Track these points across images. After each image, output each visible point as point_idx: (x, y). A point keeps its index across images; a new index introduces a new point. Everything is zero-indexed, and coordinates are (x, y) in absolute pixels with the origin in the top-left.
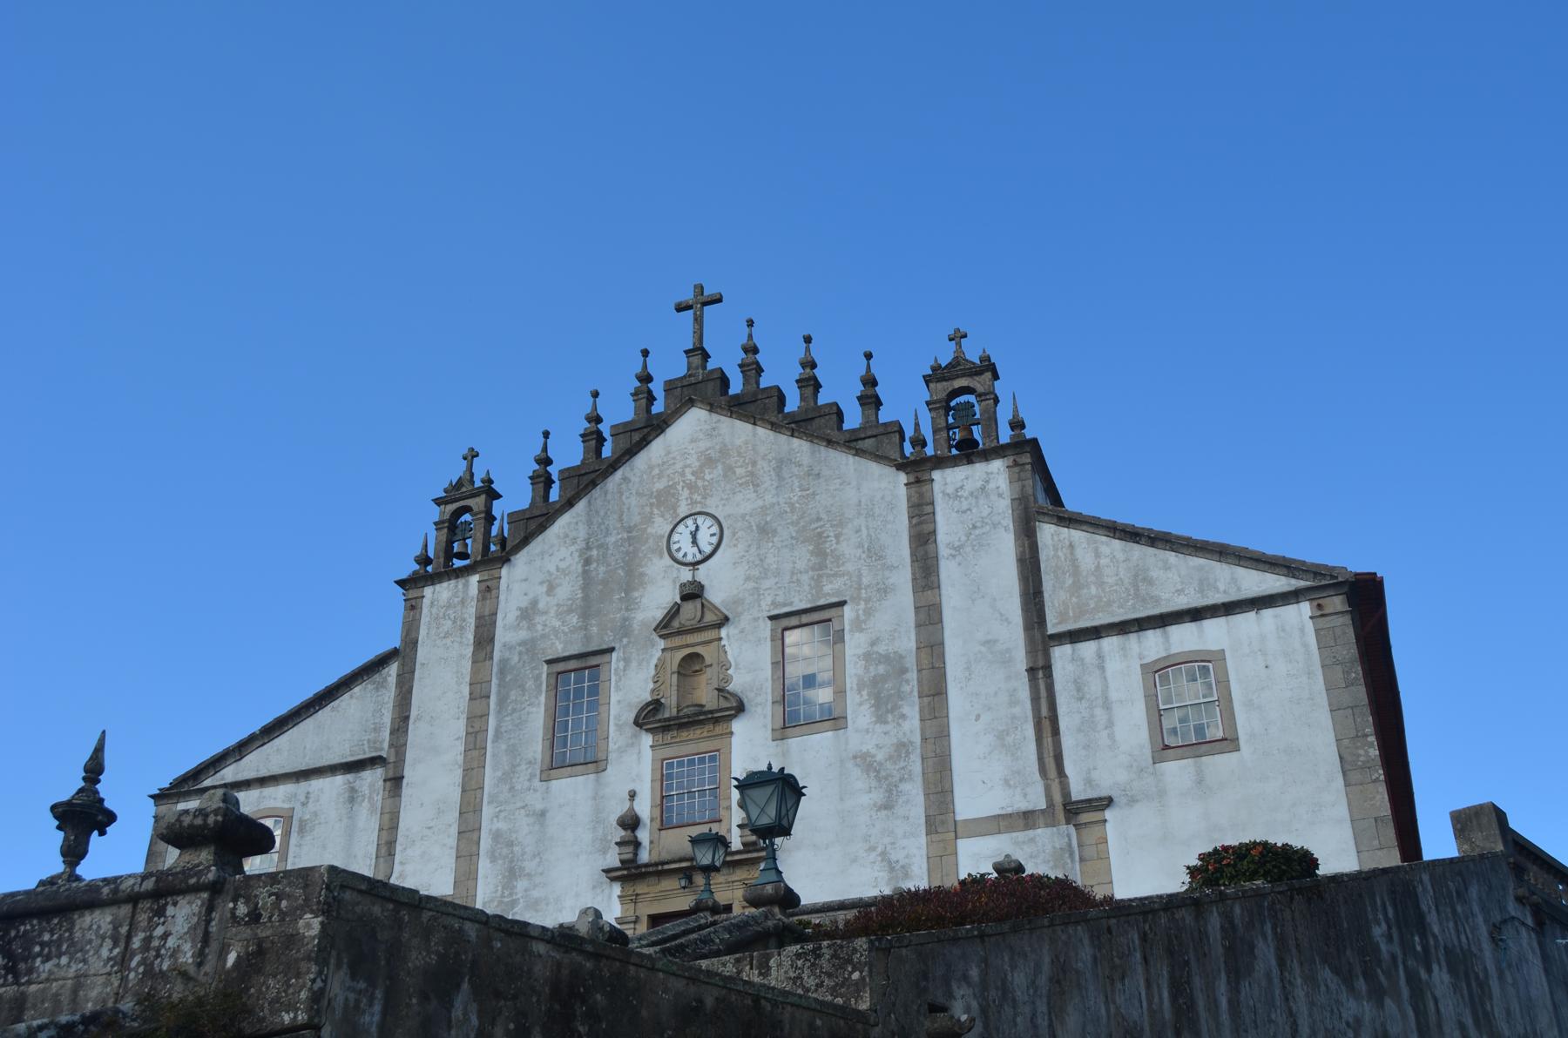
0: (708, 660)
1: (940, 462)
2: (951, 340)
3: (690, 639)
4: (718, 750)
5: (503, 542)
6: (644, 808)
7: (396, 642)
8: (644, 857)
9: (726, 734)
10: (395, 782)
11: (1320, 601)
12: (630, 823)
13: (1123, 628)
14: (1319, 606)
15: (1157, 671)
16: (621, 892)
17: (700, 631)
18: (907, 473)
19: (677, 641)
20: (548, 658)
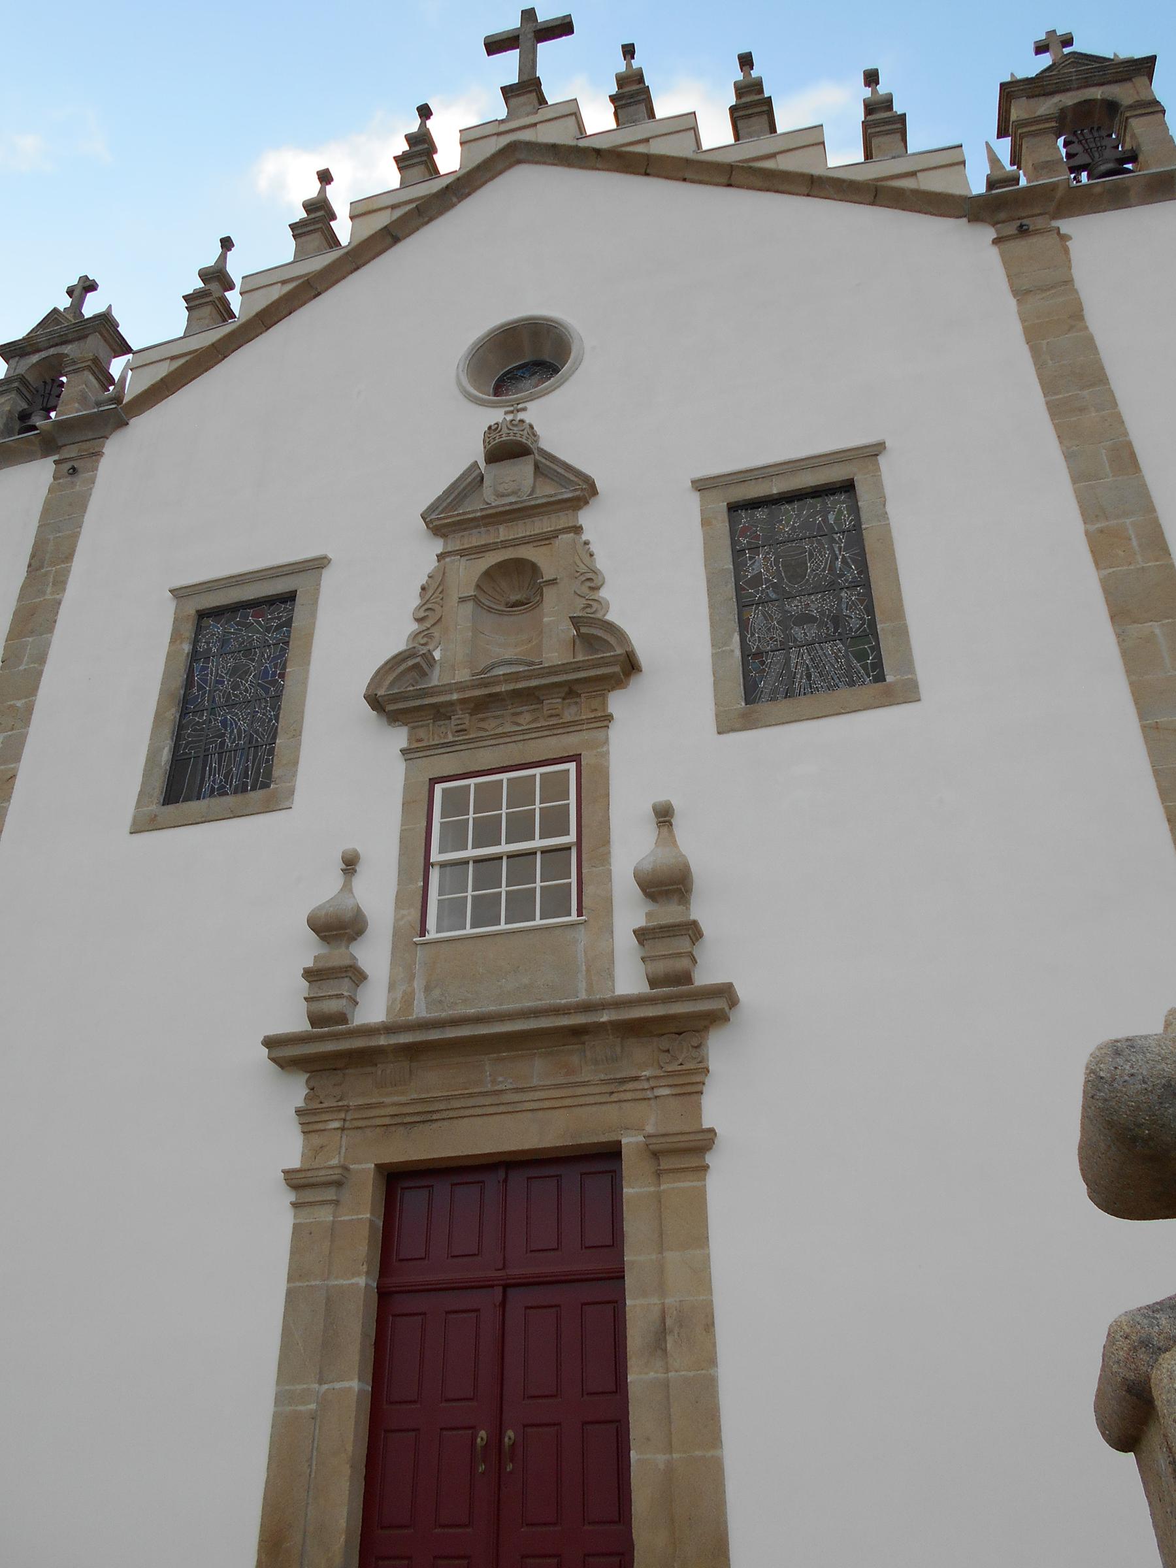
0: (548, 573)
3: (504, 533)
4: (576, 758)
9: (597, 719)
16: (307, 1098)
17: (530, 516)
19: (476, 538)
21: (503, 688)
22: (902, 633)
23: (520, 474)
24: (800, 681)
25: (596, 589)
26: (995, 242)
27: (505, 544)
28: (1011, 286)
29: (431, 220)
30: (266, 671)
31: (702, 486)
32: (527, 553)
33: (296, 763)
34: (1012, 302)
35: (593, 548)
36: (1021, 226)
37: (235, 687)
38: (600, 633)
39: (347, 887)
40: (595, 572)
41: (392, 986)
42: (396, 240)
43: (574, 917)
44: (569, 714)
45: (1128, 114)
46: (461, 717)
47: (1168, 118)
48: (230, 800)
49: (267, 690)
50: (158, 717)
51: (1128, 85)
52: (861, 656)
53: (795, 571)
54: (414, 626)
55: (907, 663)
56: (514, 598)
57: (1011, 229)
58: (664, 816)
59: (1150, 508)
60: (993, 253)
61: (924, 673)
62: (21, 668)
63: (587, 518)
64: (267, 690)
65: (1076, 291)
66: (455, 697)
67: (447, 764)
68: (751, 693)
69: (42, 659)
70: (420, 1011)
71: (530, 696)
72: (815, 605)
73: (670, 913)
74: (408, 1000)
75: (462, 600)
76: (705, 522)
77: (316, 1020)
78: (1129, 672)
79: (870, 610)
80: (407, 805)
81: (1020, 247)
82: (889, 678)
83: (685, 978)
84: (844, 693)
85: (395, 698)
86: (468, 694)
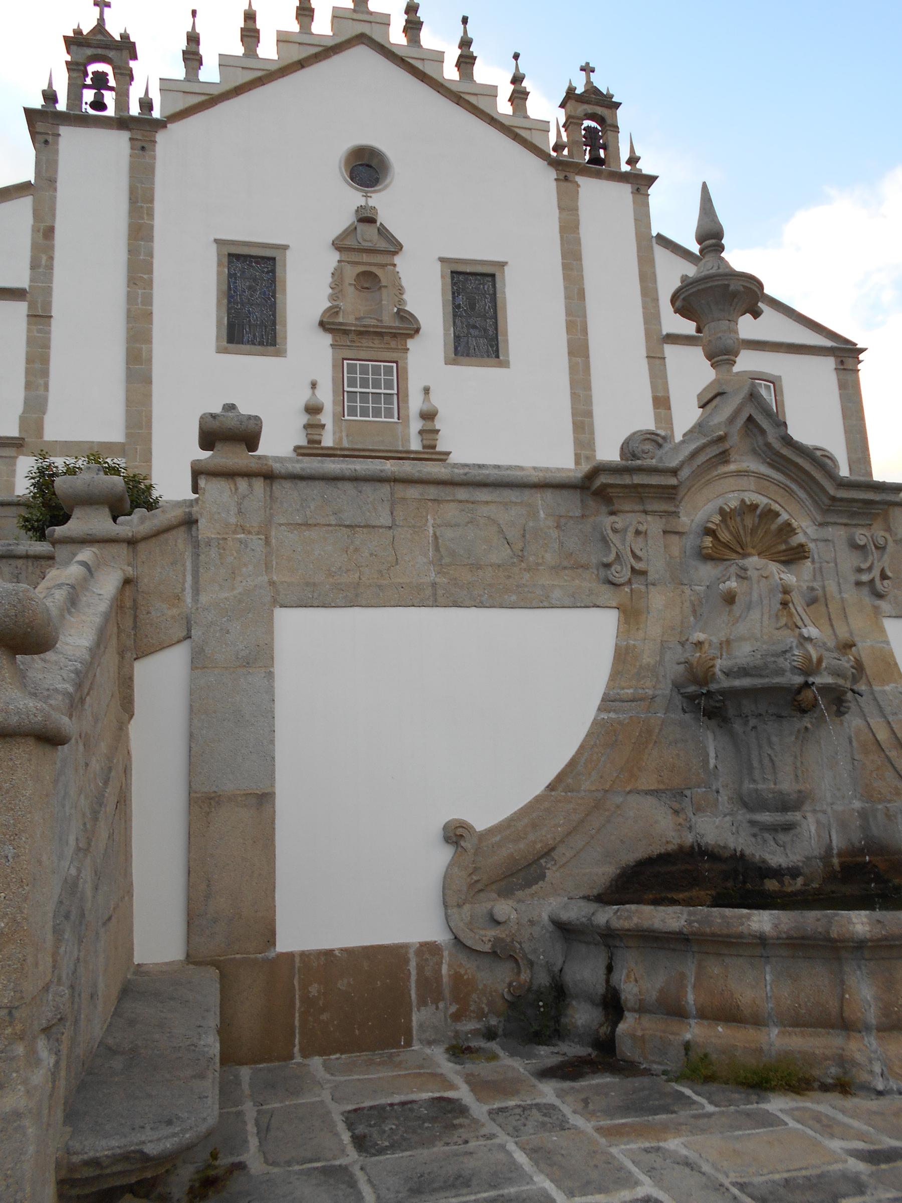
0: (384, 283)
1: (583, 170)
3: (365, 258)
4: (396, 362)
5: (146, 104)
6: (326, 396)
7: (28, 174)
8: (328, 441)
12: (313, 409)
14: (842, 362)
18: (556, 170)
19: (354, 257)
20: (218, 237)
21: (372, 330)
22: (506, 341)
24: (472, 351)
25: (401, 294)
26: (556, 180)
28: (559, 204)
29: (320, 61)
30: (265, 294)
31: (442, 260)
32: (374, 269)
33: (286, 338)
34: (557, 211)
35: (401, 275)
36: (566, 176)
38: (408, 317)
39: (314, 394)
40: (402, 287)
41: (334, 433)
42: (303, 67)
43: (396, 420)
44: (393, 344)
45: (608, 128)
46: (352, 336)
47: (619, 135)
49: (267, 302)
51: (610, 111)
52: (492, 347)
53: (472, 306)
54: (330, 291)
55: (507, 355)
56: (365, 285)
57: (562, 177)
58: (427, 390)
59: (585, 316)
60: (554, 184)
61: (512, 358)
63: (397, 260)
64: (267, 302)
65: (578, 215)
66: (353, 328)
67: (348, 353)
68: (456, 352)
69: (151, 255)
70: (345, 444)
72: (478, 322)
73: (429, 426)
74: (341, 439)
75: (350, 284)
76: (442, 277)
77: (309, 442)
78: (570, 373)
79: (496, 329)
80: (334, 366)
81: (564, 184)
82: (501, 358)
83: (434, 447)
84: (486, 360)
85: (329, 323)
86: (359, 329)
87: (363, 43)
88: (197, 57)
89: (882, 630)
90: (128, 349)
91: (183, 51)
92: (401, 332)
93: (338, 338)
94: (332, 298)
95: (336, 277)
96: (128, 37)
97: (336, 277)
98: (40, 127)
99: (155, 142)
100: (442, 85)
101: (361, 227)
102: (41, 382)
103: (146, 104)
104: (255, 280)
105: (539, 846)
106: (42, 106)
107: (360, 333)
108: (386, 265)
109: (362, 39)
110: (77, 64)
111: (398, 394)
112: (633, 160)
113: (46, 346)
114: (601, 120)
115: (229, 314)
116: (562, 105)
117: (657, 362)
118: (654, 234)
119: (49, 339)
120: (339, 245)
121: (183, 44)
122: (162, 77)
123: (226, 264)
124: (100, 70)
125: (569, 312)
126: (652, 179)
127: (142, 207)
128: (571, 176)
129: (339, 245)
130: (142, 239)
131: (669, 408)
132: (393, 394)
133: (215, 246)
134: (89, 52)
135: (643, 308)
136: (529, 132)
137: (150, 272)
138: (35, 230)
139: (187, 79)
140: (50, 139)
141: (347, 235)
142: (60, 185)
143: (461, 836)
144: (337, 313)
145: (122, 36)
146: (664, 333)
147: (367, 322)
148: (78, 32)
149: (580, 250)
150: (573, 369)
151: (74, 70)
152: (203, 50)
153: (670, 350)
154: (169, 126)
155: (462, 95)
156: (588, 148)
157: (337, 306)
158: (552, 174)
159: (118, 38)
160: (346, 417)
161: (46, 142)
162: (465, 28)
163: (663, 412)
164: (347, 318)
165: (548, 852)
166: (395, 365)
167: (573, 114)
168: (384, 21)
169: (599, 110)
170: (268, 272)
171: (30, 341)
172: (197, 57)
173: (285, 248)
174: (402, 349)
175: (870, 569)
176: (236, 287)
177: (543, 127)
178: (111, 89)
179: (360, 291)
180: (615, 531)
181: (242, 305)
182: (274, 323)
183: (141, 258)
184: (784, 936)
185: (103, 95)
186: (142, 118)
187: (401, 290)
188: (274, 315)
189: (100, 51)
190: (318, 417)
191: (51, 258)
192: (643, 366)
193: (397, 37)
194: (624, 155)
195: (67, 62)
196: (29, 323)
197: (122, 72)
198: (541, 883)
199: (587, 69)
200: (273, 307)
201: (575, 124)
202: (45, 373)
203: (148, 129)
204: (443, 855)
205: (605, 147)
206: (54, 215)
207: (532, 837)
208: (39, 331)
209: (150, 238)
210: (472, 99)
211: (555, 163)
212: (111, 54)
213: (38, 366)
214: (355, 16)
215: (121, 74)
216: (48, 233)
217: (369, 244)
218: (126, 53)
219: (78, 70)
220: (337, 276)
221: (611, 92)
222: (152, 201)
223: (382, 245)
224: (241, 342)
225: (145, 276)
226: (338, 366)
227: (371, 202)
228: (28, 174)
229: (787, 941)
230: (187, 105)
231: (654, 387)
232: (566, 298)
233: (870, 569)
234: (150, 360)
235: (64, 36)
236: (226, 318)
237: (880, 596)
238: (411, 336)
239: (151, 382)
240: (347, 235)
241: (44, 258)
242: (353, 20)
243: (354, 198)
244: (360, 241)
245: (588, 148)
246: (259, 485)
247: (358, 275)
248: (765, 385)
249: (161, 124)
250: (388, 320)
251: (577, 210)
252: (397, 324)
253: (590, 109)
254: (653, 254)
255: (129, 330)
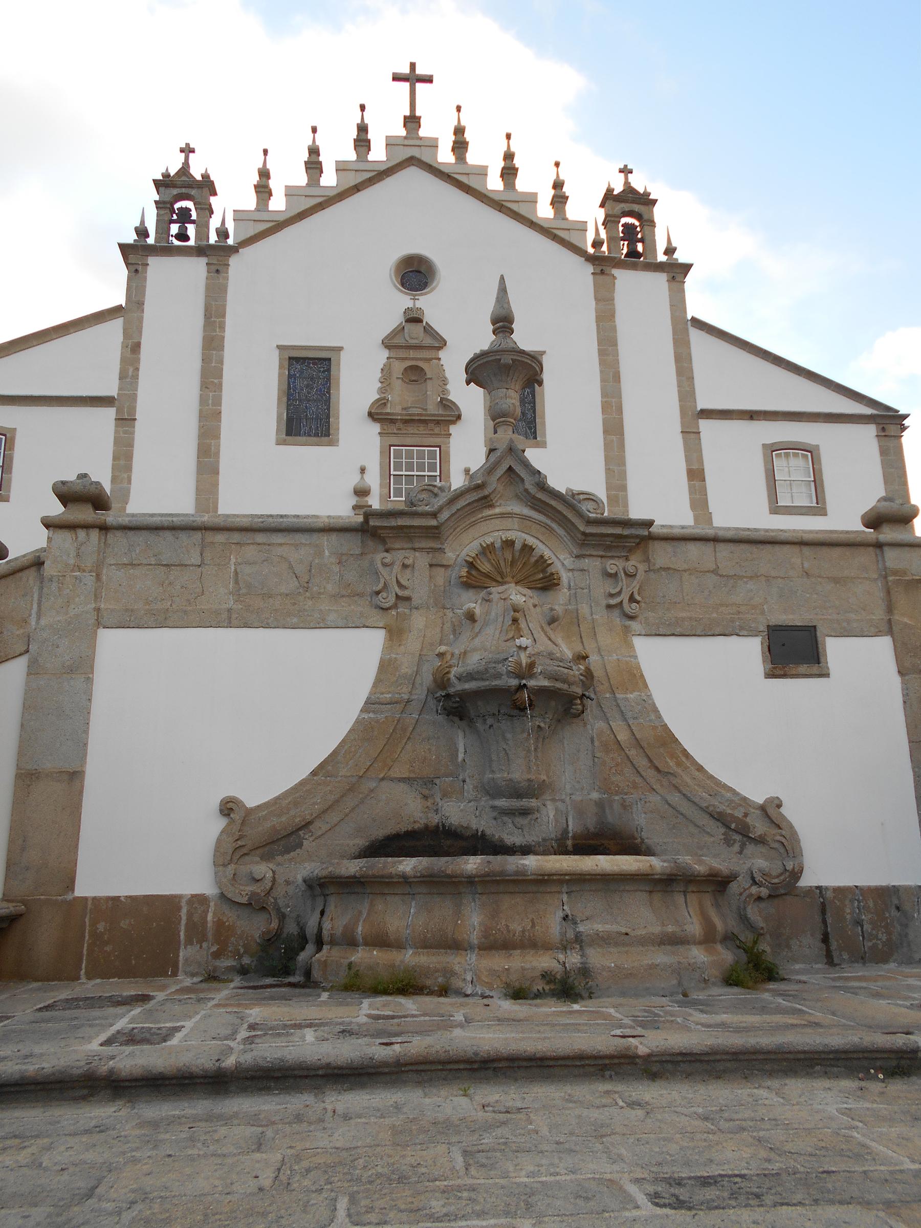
2: (620, 172)
3: (412, 354)
4: (439, 447)
5: (223, 233)
6: (373, 480)
7: (120, 299)
9: (446, 434)
10: (126, 420)
11: (884, 426)
13: (752, 415)
15: (772, 450)
19: (402, 354)
21: (417, 418)
22: (544, 424)
23: (417, 329)
25: (446, 385)
27: (413, 359)
28: (595, 296)
32: (420, 364)
34: (594, 303)
35: (445, 367)
37: (309, 393)
38: (450, 405)
39: (362, 478)
44: (437, 430)
48: (315, 439)
49: (322, 397)
50: (279, 399)
52: (530, 428)
54: (380, 385)
55: (544, 435)
56: (413, 378)
57: (598, 271)
60: (591, 277)
61: (549, 439)
62: (213, 365)
63: (441, 354)
67: (394, 440)
69: (221, 362)
71: (425, 422)
75: (397, 378)
78: (605, 451)
85: (377, 414)
86: (404, 418)
87: (413, 165)
88: (266, 190)
89: (631, 646)
90: (199, 444)
91: (255, 185)
92: (443, 418)
93: (385, 427)
94: (381, 390)
95: (385, 372)
96: (208, 177)
97: (385, 372)
98: (132, 258)
99: (228, 265)
100: (485, 196)
101: (409, 327)
102: (126, 476)
103: (223, 233)
104: (312, 379)
105: (297, 820)
106: (135, 240)
107: (406, 422)
108: (431, 359)
109: (412, 161)
110: (164, 202)
111: (440, 476)
112: (670, 251)
113: (130, 445)
114: (638, 217)
115: (288, 410)
116: (602, 205)
117: (693, 436)
118: (689, 318)
119: (133, 439)
120: (388, 343)
121: (256, 178)
122: (235, 209)
123: (287, 366)
124: (184, 206)
125: (604, 394)
126: (687, 268)
127: (215, 322)
128: (606, 269)
129: (388, 343)
130: (214, 349)
131: (704, 480)
132: (436, 476)
133: (277, 352)
134: (175, 191)
135: (679, 386)
136: (567, 232)
137: (220, 376)
138: (124, 346)
139: (258, 210)
140: (140, 268)
141: (395, 335)
142: (147, 307)
143: (232, 809)
144: (385, 404)
145: (202, 176)
146: (699, 409)
147: (412, 411)
148: (166, 175)
149: (616, 337)
150: (607, 446)
151: (161, 208)
152: (272, 183)
153: (705, 425)
154: (240, 250)
155: (504, 203)
156: (626, 243)
157: (384, 398)
158: (590, 269)
159: (199, 178)
160: (392, 498)
161: (136, 271)
162: (508, 142)
163: (697, 483)
164: (394, 409)
165: (307, 824)
166: (438, 449)
167: (610, 213)
168: (433, 145)
169: (636, 208)
170: (324, 372)
171: (117, 441)
172: (266, 190)
173: (339, 349)
174: (444, 435)
175: (620, 593)
176: (295, 386)
177: (581, 227)
178: (193, 222)
179: (407, 383)
180: (385, 565)
181: (300, 401)
182: (328, 417)
183: (213, 365)
184: (419, 875)
185: (186, 228)
186: (218, 246)
187: (445, 382)
188: (329, 409)
189: (184, 190)
190: (366, 499)
191: (137, 369)
192: (678, 441)
193: (445, 156)
194: (661, 247)
195: (156, 202)
196: (116, 426)
197: (203, 206)
198: (298, 851)
199: (626, 171)
200: (328, 402)
201: (613, 222)
202: (128, 468)
203: (222, 254)
204: (218, 824)
205: (642, 240)
206: (140, 332)
207: (292, 813)
208: (125, 432)
209: (221, 348)
210: (514, 207)
211: (591, 259)
212: (193, 192)
213: (122, 462)
214: (406, 142)
215: (201, 209)
216: (135, 348)
217: (417, 341)
218: (206, 191)
219: (165, 208)
220: (386, 372)
221: (648, 190)
222: (224, 316)
223: (428, 341)
224: (298, 434)
225: (216, 381)
226: (385, 452)
227: (419, 304)
228: (120, 299)
229: (422, 879)
230: (257, 231)
231: (688, 460)
232: (602, 381)
233: (620, 593)
234: (217, 454)
235: (153, 180)
236: (285, 414)
237: (631, 618)
238: (454, 422)
239: (218, 473)
240: (395, 335)
241: (131, 370)
242: (404, 145)
243: (404, 301)
244: (408, 338)
245: (626, 243)
246: (95, 534)
247: (406, 369)
248: (802, 454)
249: (234, 250)
250: (432, 408)
251: (613, 300)
252: (441, 412)
253: (627, 207)
254: (688, 336)
255: (201, 427)
